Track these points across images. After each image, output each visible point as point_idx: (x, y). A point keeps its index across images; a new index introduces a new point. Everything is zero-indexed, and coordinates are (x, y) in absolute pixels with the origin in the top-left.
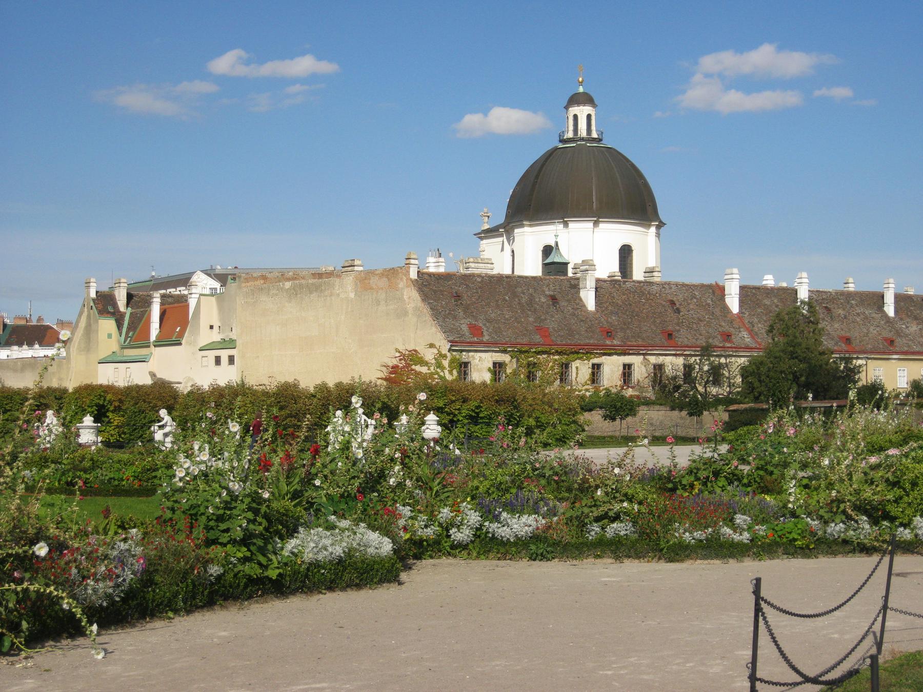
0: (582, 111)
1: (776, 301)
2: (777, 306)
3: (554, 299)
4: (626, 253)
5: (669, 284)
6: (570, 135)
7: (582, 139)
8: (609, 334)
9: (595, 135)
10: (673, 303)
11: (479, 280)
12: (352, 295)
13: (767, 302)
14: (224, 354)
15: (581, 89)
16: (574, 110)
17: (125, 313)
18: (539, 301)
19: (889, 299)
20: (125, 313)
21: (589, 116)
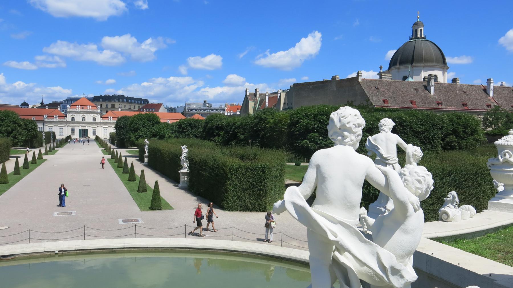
1: (507, 92)
2: (508, 94)
3: (416, 90)
5: (463, 85)
7: (418, 38)
9: (423, 36)
11: (386, 82)
12: (335, 89)
16: (416, 28)
17: (258, 100)
18: (411, 91)
20: (258, 100)
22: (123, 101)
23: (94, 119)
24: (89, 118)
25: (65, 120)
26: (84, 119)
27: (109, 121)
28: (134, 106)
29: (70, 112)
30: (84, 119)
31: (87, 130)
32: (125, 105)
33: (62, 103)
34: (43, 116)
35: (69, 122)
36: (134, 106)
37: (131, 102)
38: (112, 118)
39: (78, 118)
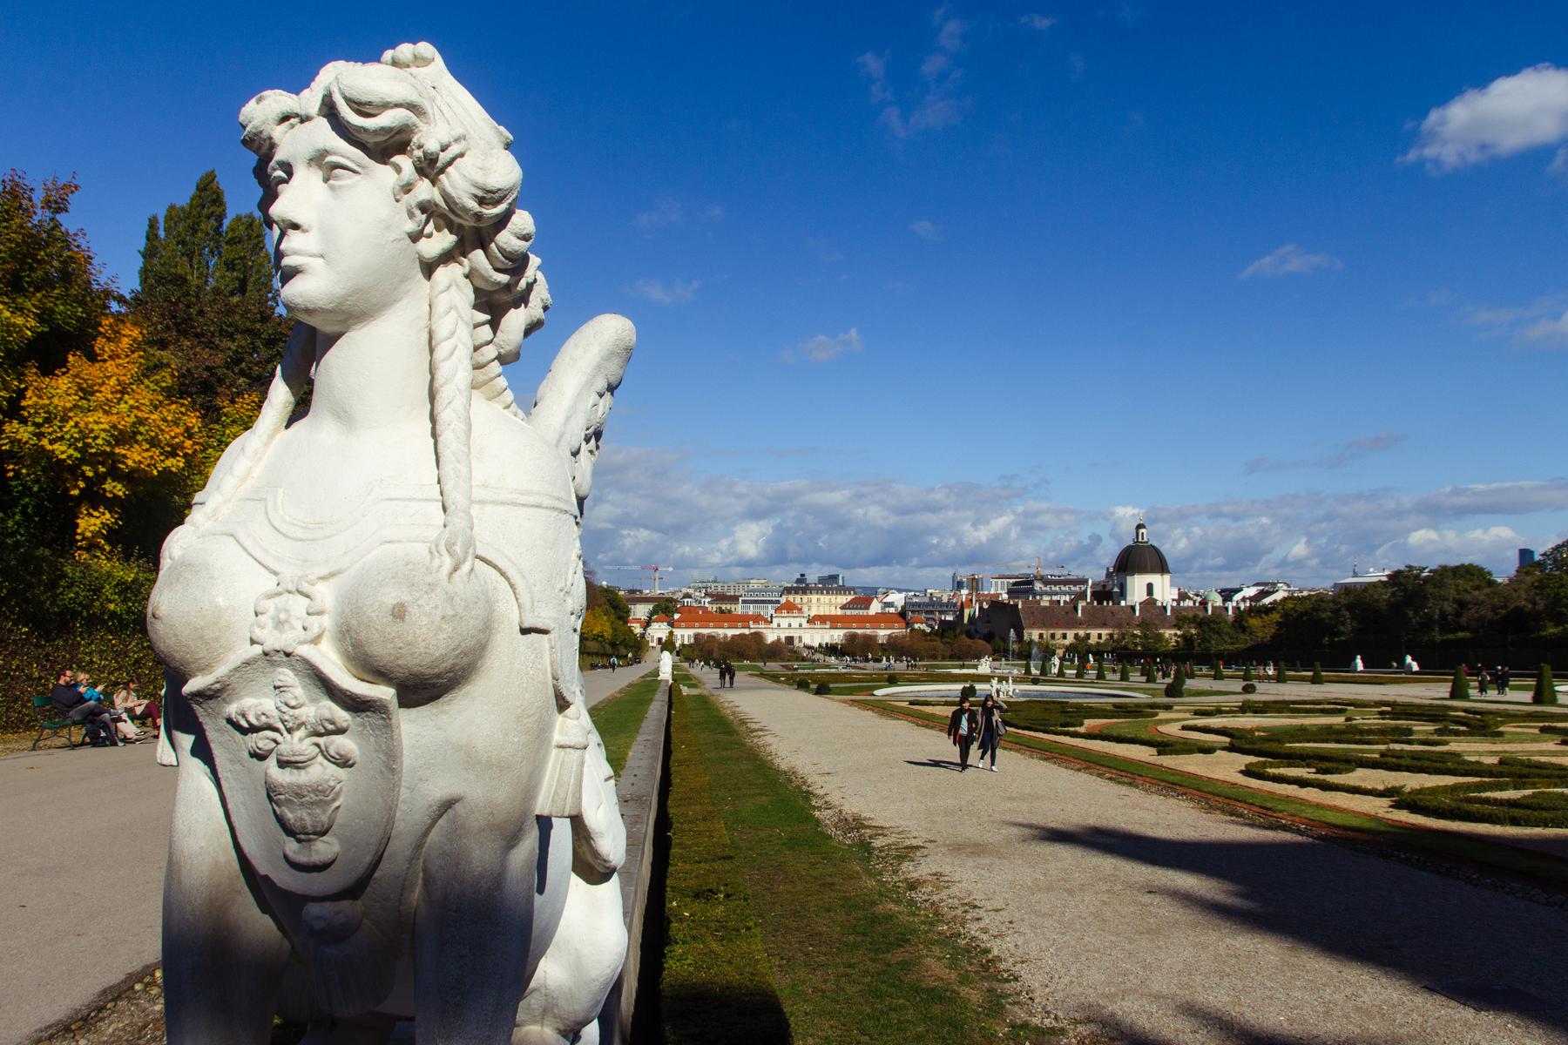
4: (1150, 587)
9: (1145, 539)
22: (822, 593)
23: (800, 625)
24: (795, 623)
26: (790, 625)
30: (790, 625)
37: (833, 593)
39: (784, 623)
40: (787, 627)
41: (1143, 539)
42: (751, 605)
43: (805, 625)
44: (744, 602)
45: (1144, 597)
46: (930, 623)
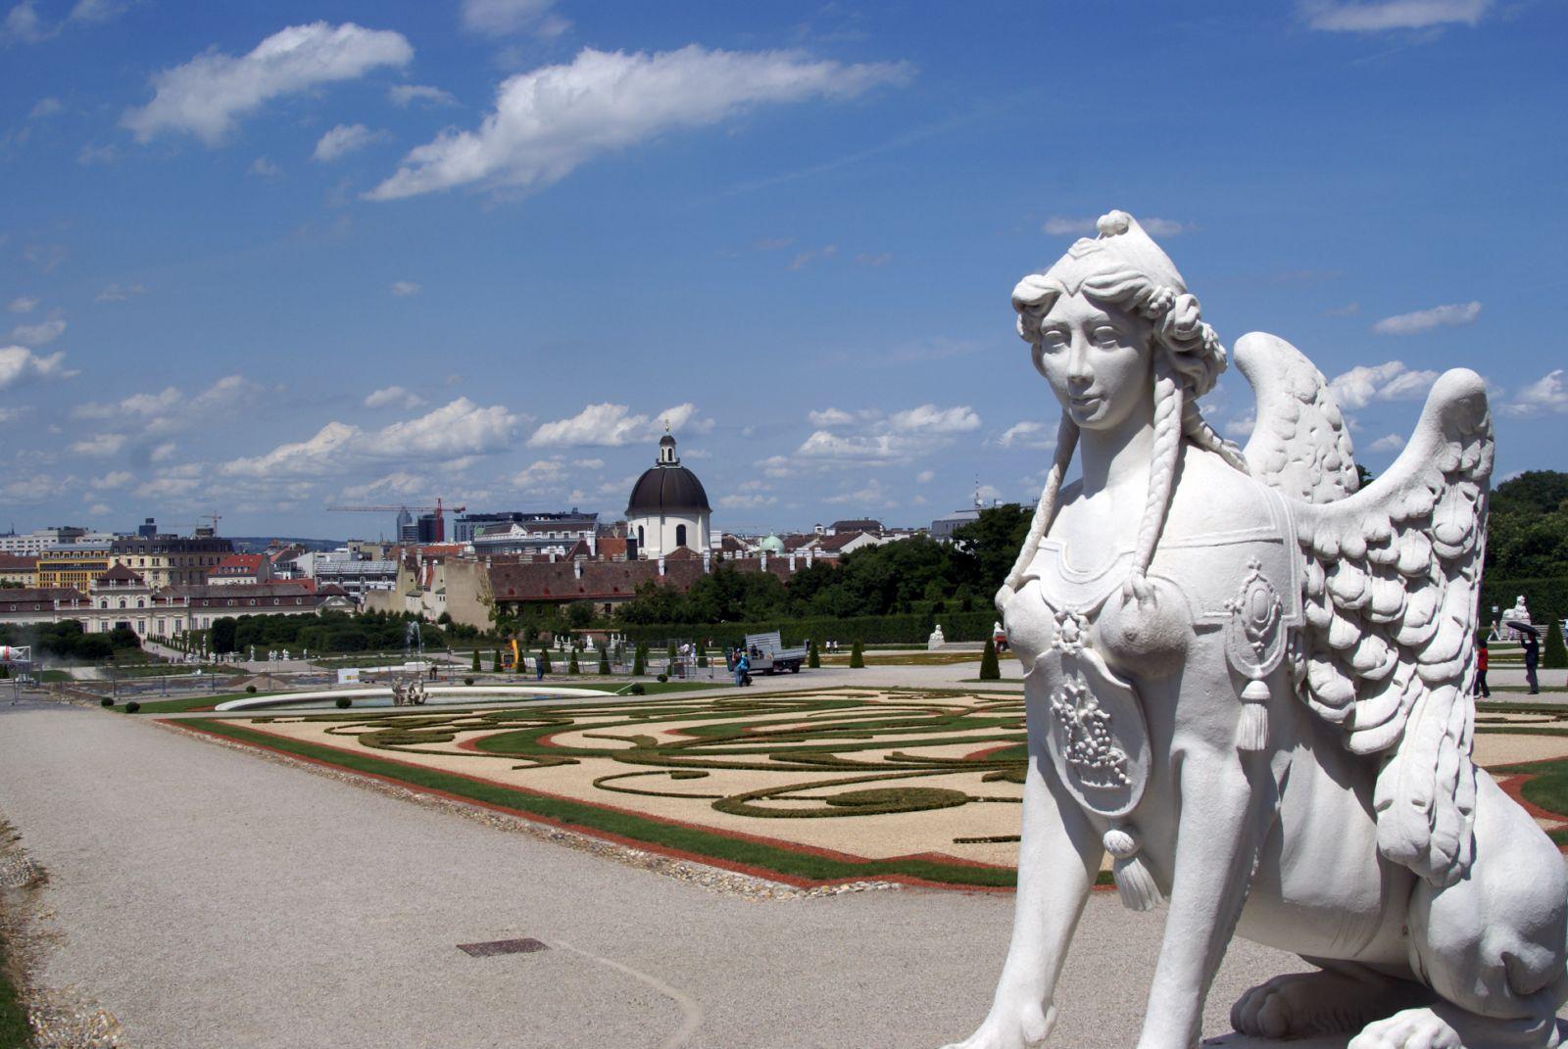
0: (666, 449)
4: (681, 530)
6: (660, 461)
7: (665, 464)
8: (582, 590)
9: (674, 461)
10: (627, 572)
13: (685, 568)
14: (442, 596)
15: (668, 434)
19: (764, 562)
21: (670, 451)
22: (178, 551)
23: (141, 603)
24: (132, 602)
25: (91, 608)
26: (123, 604)
27: (167, 606)
28: (201, 560)
29: (99, 593)
30: (123, 604)
31: (129, 623)
32: (181, 559)
33: (39, 558)
34: (52, 602)
35: (97, 612)
36: (201, 560)
38: (174, 599)
39: (114, 603)
40: (118, 607)
41: (670, 459)
42: (58, 574)
43: (148, 603)
44: (44, 567)
45: (671, 546)
46: (353, 594)
